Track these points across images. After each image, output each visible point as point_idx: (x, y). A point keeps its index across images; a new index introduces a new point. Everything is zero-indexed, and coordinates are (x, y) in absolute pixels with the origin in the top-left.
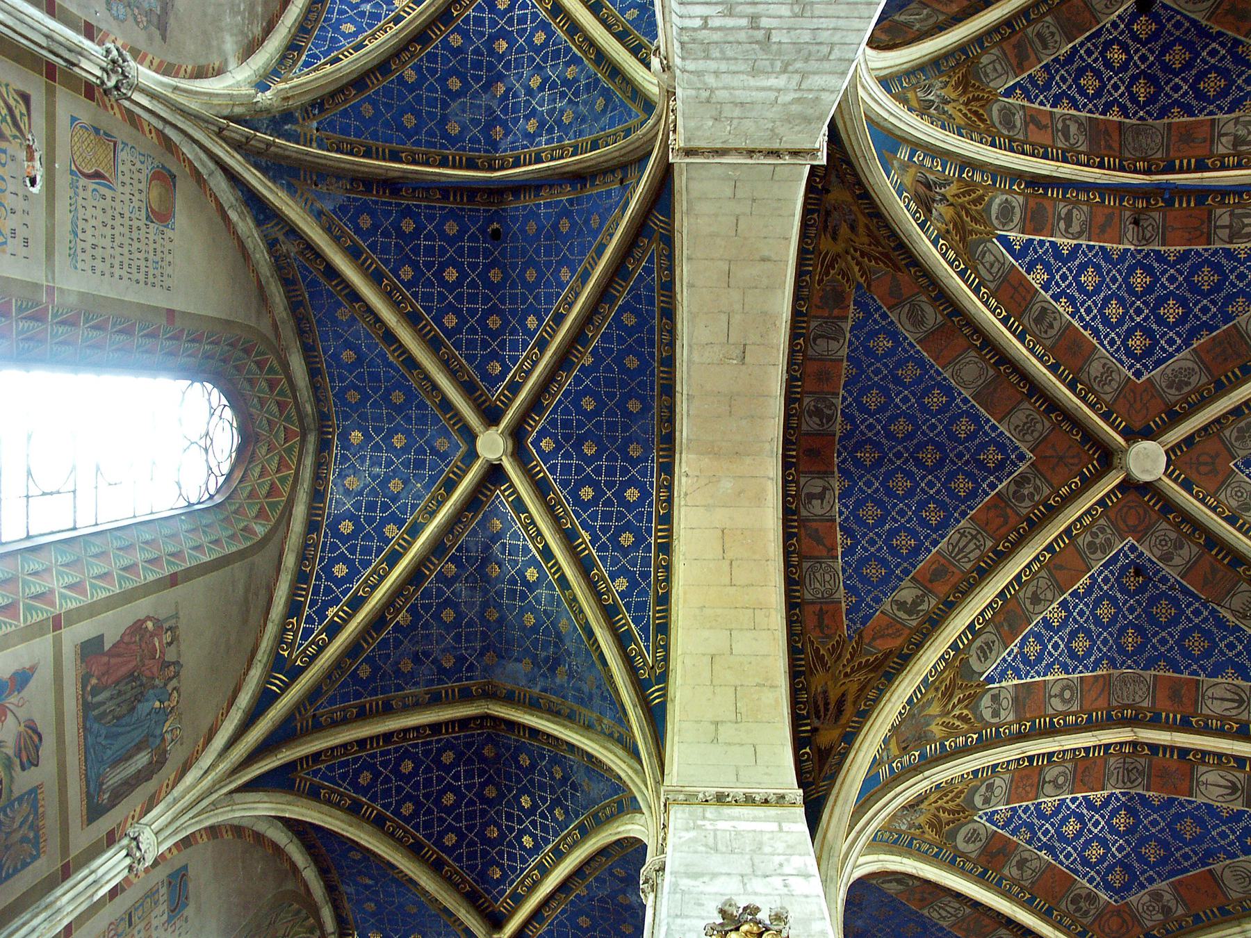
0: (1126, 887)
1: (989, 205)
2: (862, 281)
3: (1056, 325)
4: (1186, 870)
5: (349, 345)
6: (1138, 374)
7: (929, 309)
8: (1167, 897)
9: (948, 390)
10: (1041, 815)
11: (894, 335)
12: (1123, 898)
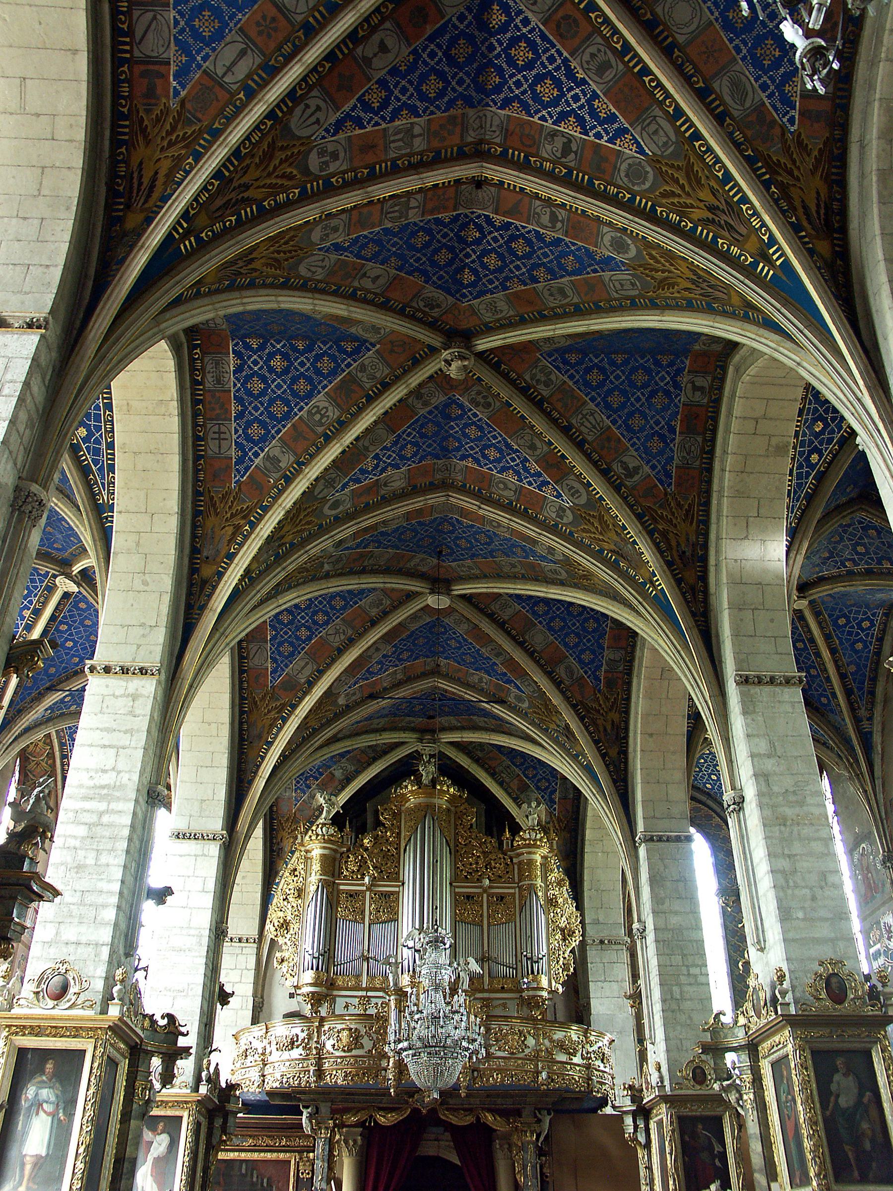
0: (447, 405)
1: (529, 708)
2: (598, 695)
3: (489, 649)
4: (408, 427)
5: (856, 652)
6: (438, 619)
7: (563, 675)
8: (420, 406)
9: (550, 629)
10: (518, 473)
11: (581, 661)
12: (449, 398)
